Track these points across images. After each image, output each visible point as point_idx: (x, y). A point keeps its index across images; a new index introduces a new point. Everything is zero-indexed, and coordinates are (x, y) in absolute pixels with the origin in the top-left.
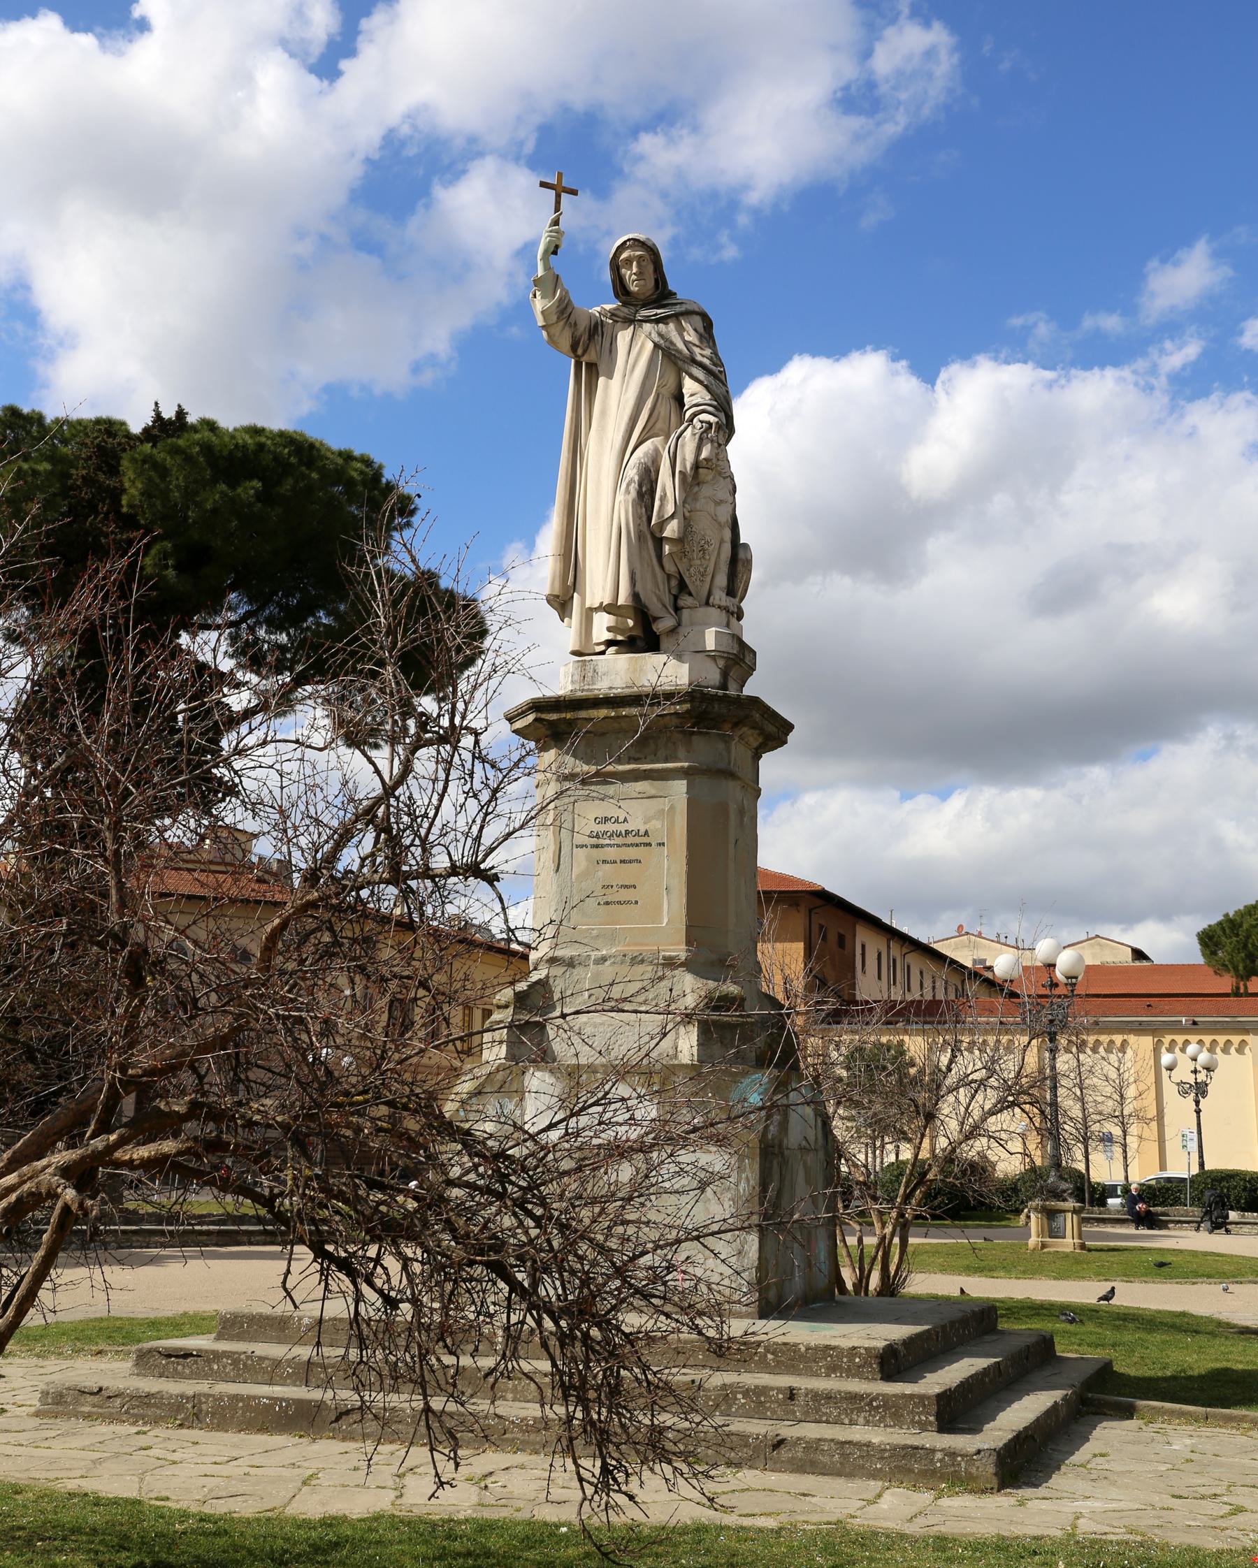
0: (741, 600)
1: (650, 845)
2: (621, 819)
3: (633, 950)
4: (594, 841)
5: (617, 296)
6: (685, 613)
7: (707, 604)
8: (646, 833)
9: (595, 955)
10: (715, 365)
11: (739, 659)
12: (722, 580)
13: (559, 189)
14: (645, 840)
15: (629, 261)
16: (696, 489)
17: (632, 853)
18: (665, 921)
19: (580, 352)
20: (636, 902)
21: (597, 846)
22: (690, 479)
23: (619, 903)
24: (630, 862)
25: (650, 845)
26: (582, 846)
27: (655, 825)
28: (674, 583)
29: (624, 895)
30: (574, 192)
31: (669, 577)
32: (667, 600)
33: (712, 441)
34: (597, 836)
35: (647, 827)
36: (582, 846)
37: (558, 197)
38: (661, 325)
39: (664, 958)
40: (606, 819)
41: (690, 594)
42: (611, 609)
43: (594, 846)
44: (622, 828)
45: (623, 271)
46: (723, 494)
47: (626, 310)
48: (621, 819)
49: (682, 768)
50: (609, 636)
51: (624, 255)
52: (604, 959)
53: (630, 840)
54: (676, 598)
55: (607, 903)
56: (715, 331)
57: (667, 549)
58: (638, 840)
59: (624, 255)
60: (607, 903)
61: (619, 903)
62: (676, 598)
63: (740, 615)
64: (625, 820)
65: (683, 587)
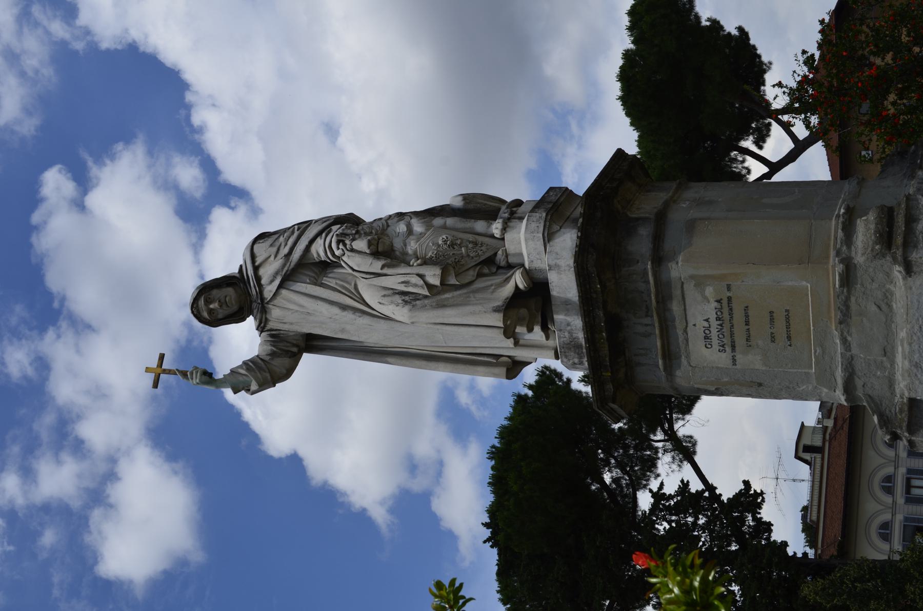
0: (503, 202)
1: (729, 299)
3: (835, 316)
4: (728, 349)
5: (243, 319)
6: (512, 260)
7: (503, 239)
8: (719, 301)
9: (839, 348)
10: (293, 233)
11: (555, 206)
12: (480, 226)
13: (159, 370)
14: (725, 302)
15: (211, 311)
16: (397, 253)
18: (804, 283)
19: (295, 350)
20: (787, 311)
21: (733, 347)
22: (389, 261)
23: (788, 327)
24: (747, 316)
25: (729, 299)
28: (486, 271)
29: (780, 324)
31: (480, 275)
33: (353, 240)
35: (712, 300)
37: (165, 371)
38: (263, 282)
39: (841, 286)
40: (706, 338)
41: (496, 254)
42: (509, 332)
43: (733, 347)
44: (715, 324)
45: (220, 316)
46: (402, 227)
47: (255, 311)
49: (653, 268)
50: (537, 329)
51: (205, 314)
52: (844, 341)
53: (726, 316)
55: (789, 338)
56: (272, 230)
57: (453, 281)
58: (726, 310)
59: (205, 314)
60: (789, 338)
61: (788, 327)
62: (499, 267)
63: (518, 203)
64: (707, 320)
65: (490, 261)
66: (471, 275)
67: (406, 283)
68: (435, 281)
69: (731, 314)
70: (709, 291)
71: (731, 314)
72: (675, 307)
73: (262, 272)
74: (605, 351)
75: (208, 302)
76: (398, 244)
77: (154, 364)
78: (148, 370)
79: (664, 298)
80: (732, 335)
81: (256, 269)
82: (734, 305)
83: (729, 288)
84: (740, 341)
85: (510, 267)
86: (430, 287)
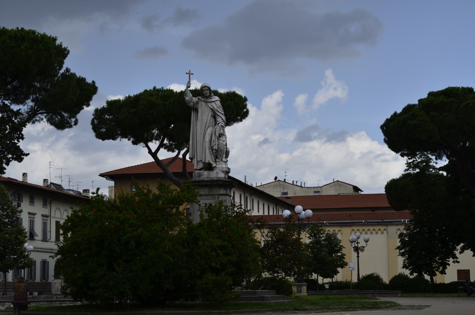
6: (217, 163)
12: (224, 156)
30: (193, 74)
32: (214, 160)
37: (190, 76)
46: (224, 139)
54: (215, 159)
57: (214, 151)
59: (204, 89)
66: (215, 154)
67: (214, 141)
68: (214, 148)
72: (210, 197)
73: (214, 103)
74: (202, 184)
75: (207, 90)
76: (221, 138)
77: (191, 73)
78: (190, 71)
79: (211, 195)
81: (214, 101)
85: (216, 162)
86: (213, 147)
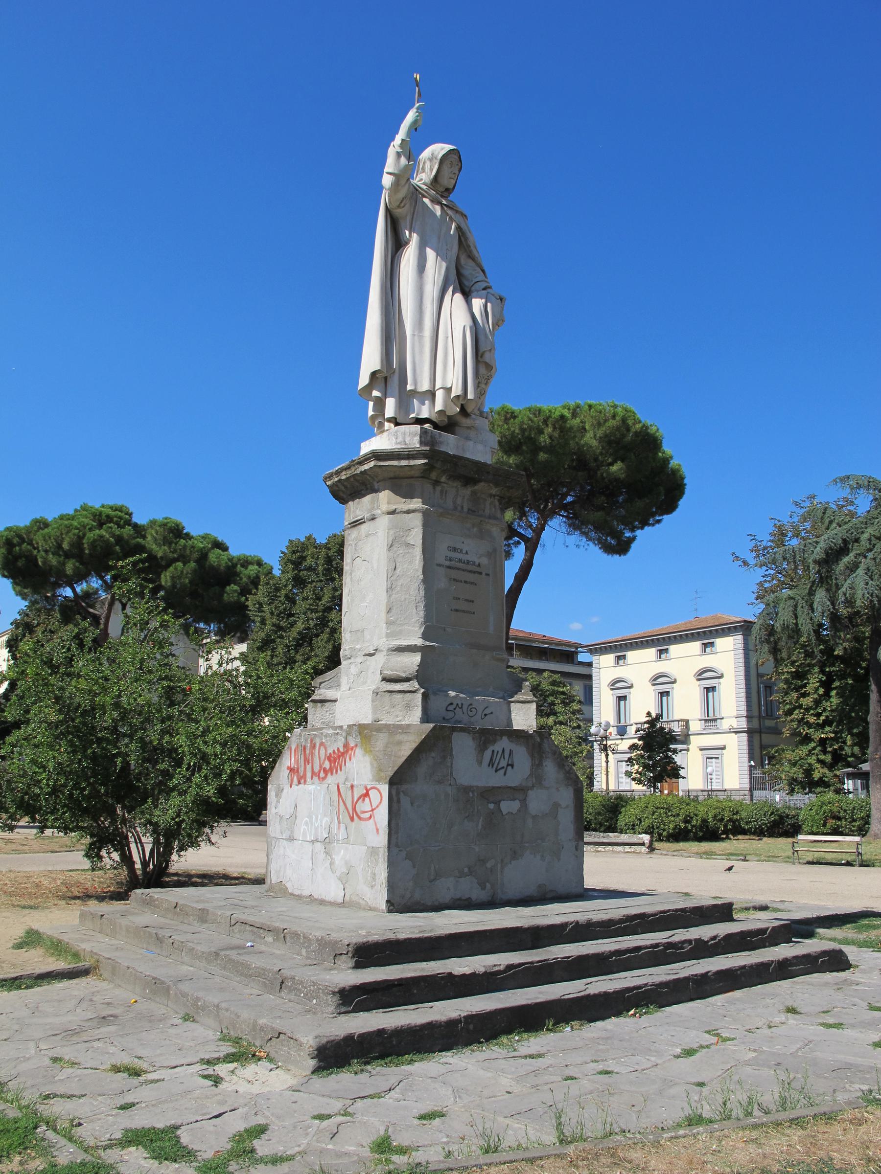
1: (481, 573)
2: (464, 551)
4: (448, 563)
8: (479, 565)
14: (478, 569)
17: (471, 577)
23: (464, 611)
25: (481, 573)
26: (440, 565)
27: (484, 561)
34: (450, 560)
36: (440, 565)
40: (455, 550)
43: (449, 567)
48: (464, 551)
53: (470, 567)
55: (457, 610)
60: (457, 610)
61: (464, 611)
64: (467, 553)
69: (470, 571)
70: (484, 561)
71: (470, 571)
80: (458, 569)
82: (477, 575)
83: (487, 575)
84: (454, 574)
